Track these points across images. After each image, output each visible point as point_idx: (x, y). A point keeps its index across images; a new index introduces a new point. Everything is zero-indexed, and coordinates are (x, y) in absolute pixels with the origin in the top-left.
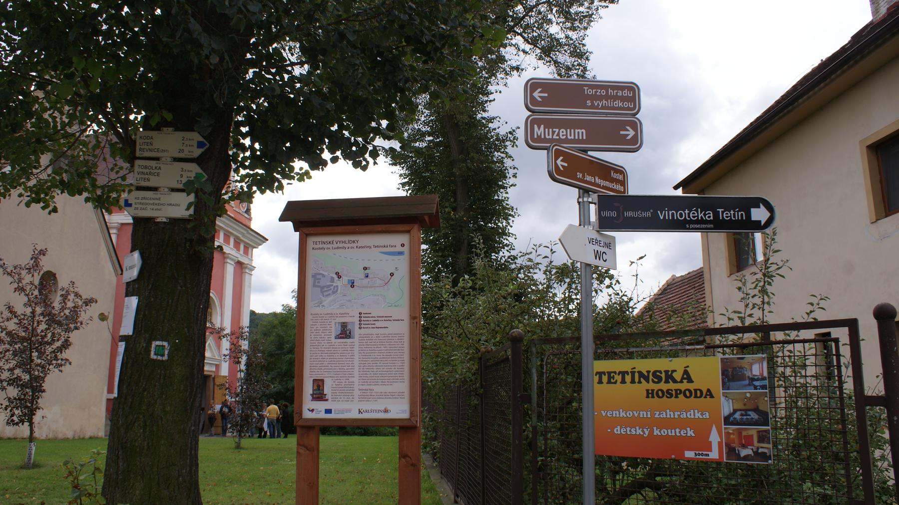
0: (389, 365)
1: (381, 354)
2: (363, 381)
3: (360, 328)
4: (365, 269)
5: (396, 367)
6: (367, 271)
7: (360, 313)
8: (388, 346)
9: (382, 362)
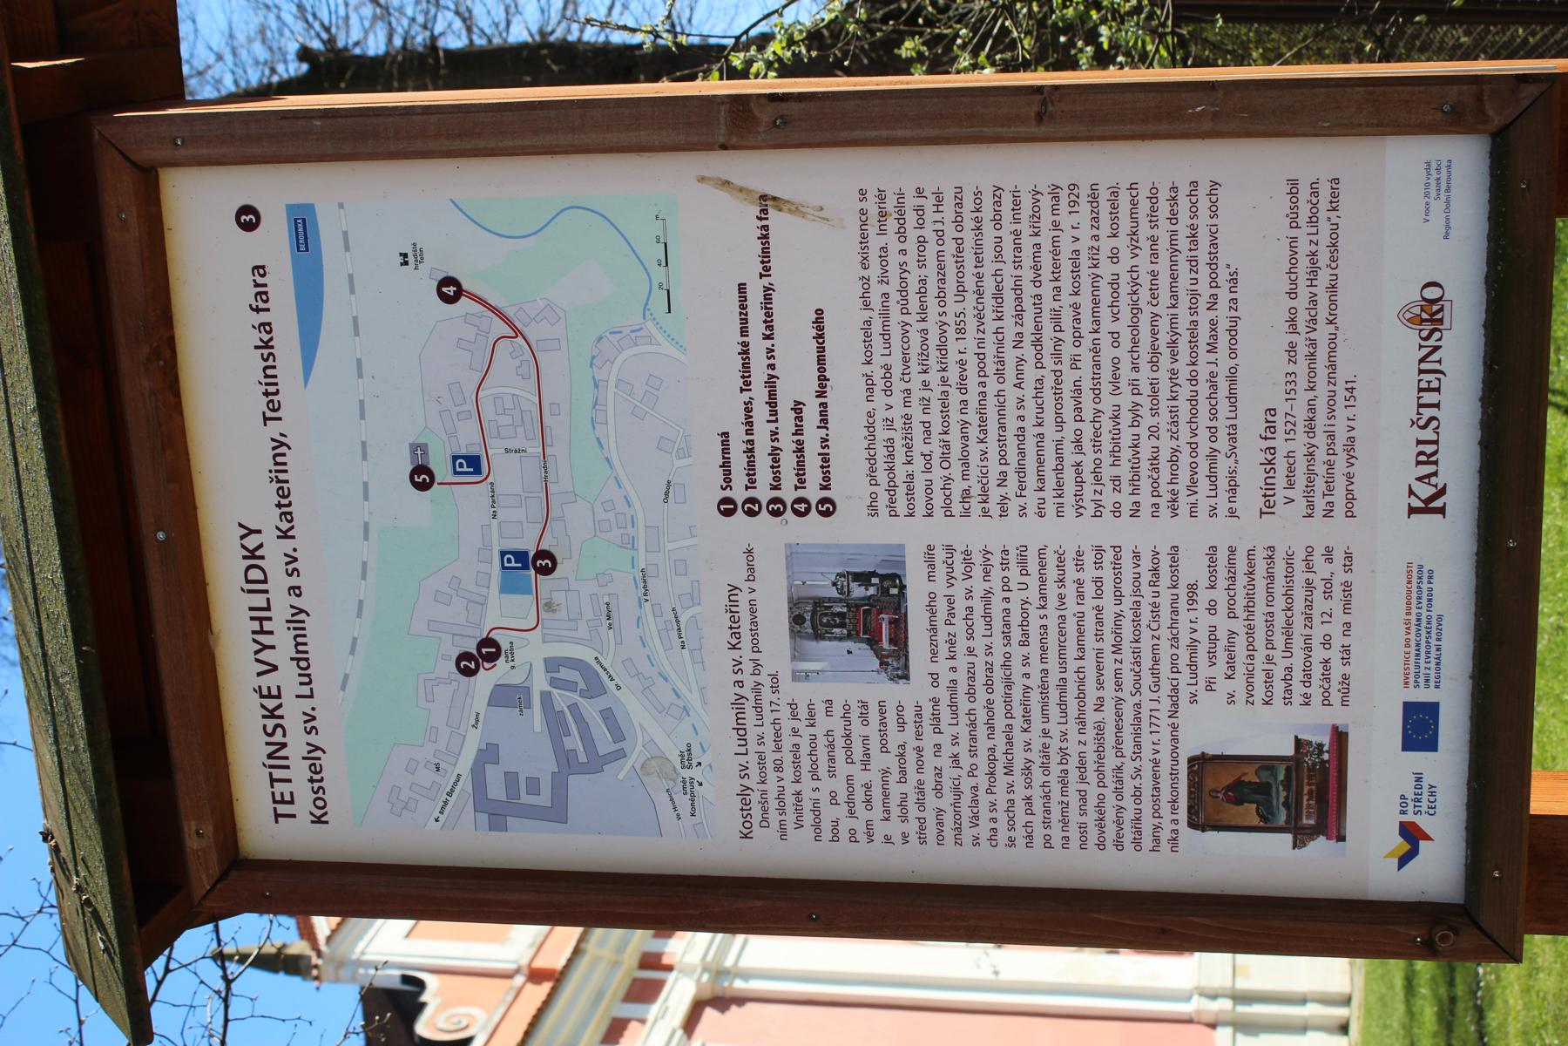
0: (1085, 299)
1: (1010, 355)
2: (1203, 485)
3: (827, 508)
4: (422, 477)
5: (1106, 245)
6: (441, 467)
7: (727, 508)
8: (952, 308)
9: (1067, 349)
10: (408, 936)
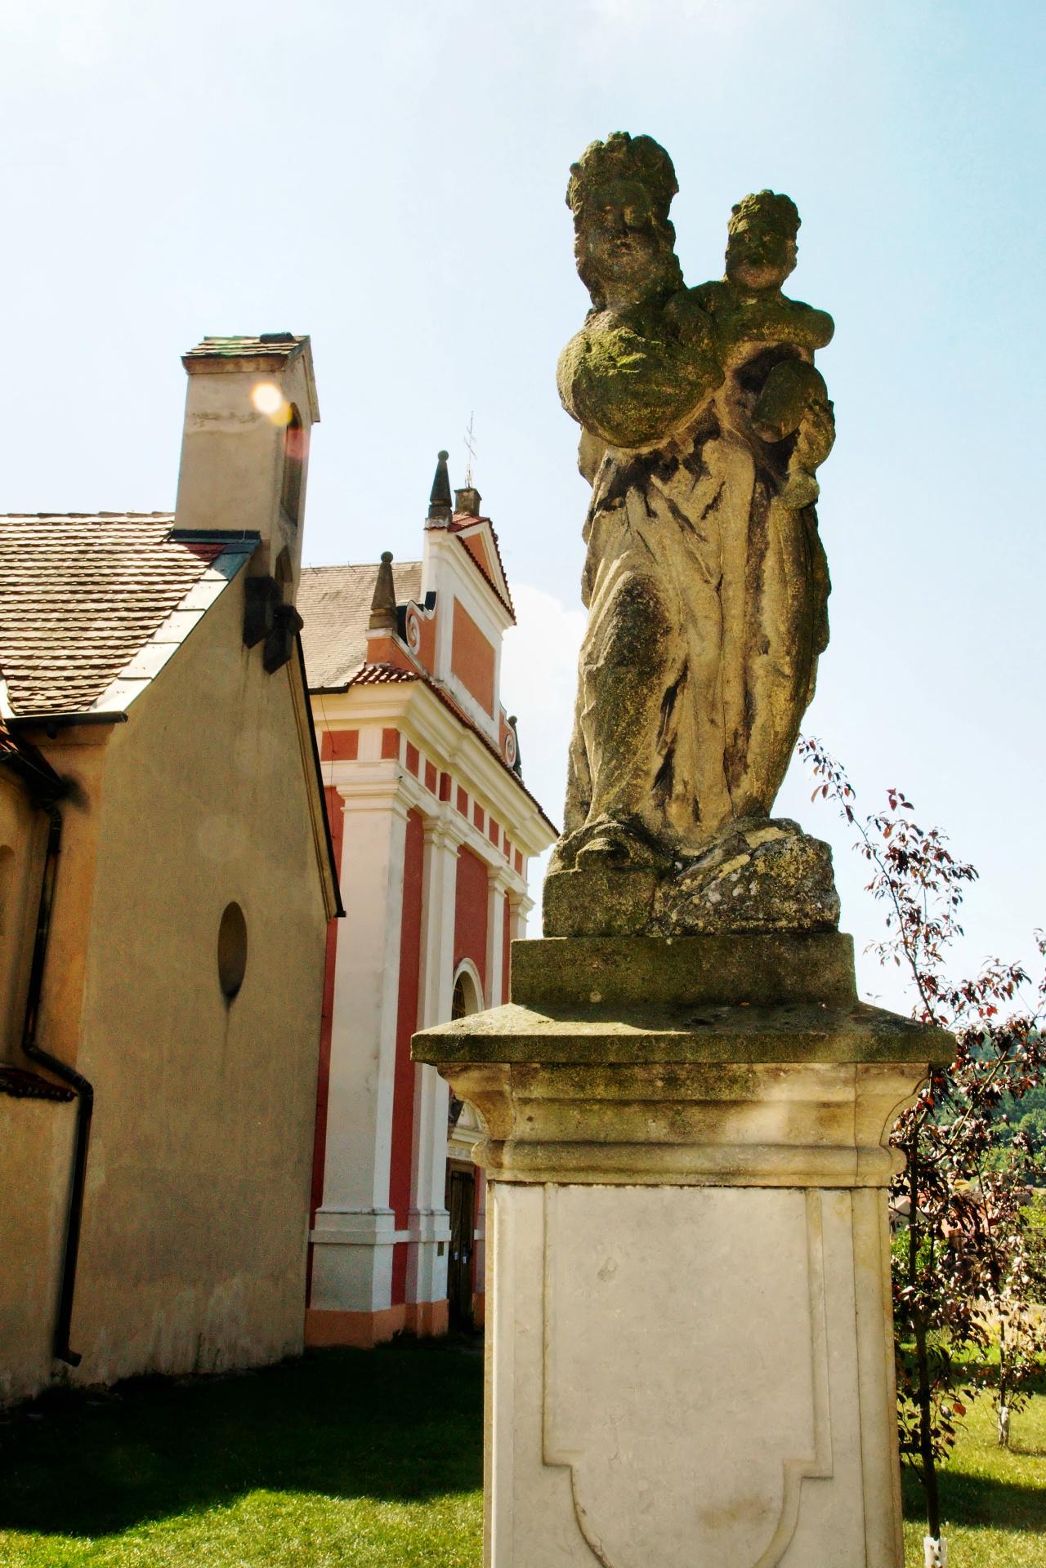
10: (456, 599)
